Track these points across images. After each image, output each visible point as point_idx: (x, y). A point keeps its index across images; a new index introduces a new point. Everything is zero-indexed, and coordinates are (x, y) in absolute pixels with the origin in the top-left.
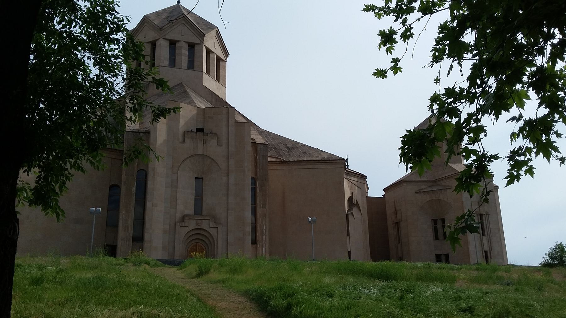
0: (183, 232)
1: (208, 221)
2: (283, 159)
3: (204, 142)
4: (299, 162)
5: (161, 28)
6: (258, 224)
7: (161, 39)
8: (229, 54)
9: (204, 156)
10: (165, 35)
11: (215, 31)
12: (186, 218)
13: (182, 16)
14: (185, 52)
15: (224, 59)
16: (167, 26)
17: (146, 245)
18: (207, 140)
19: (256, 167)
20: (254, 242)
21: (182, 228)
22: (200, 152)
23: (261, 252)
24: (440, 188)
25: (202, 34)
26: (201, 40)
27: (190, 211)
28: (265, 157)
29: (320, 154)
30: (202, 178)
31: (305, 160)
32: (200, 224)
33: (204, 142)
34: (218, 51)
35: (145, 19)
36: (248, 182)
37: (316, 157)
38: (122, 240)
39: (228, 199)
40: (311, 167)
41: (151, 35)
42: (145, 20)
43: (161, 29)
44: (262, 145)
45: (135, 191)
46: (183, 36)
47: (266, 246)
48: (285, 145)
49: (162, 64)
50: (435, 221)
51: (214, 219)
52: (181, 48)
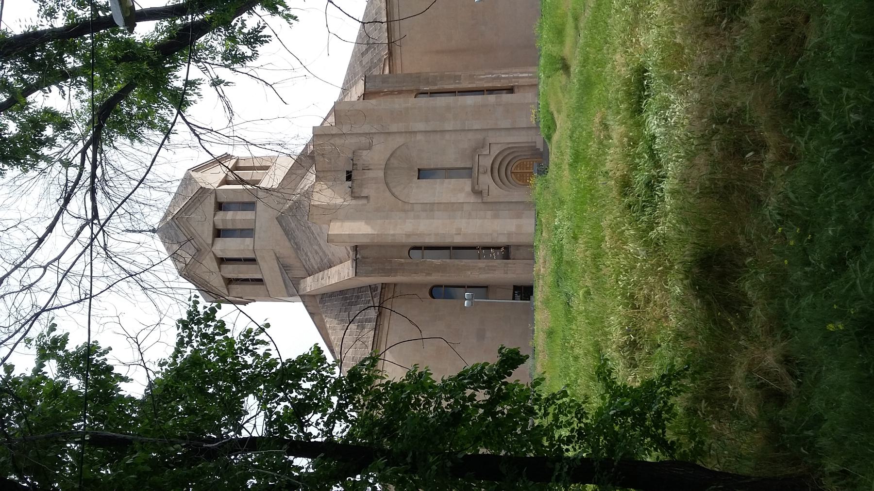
0: (496, 192)
2: (386, 55)
3: (366, 168)
5: (198, 251)
6: (485, 86)
7: (213, 249)
8: (226, 154)
9: (387, 168)
10: (208, 245)
11: (194, 174)
12: (476, 188)
14: (229, 215)
15: (235, 160)
17: (514, 240)
18: (363, 164)
19: (400, 92)
20: (511, 90)
22: (381, 174)
23: (524, 80)
25: (200, 191)
27: (466, 184)
28: (384, 79)
30: (419, 170)
32: (485, 169)
33: (366, 168)
36: (423, 101)
38: (507, 273)
41: (209, 263)
47: (516, 73)
48: (363, 54)
49: (251, 248)
52: (224, 221)
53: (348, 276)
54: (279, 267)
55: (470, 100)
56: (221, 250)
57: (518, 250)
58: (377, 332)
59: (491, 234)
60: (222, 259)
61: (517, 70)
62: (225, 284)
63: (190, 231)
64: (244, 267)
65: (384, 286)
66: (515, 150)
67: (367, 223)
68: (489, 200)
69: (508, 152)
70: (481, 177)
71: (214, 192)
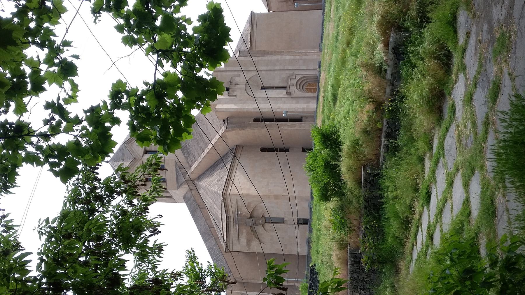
0: (298, 93)
3: (236, 84)
4: (251, 42)
7: (143, 158)
10: (140, 156)
12: (289, 91)
16: (132, 154)
33: (236, 84)
39: (277, 70)
40: (255, 34)
43: (135, 159)
45: (269, 122)
51: (289, 77)
54: (176, 169)
57: (306, 119)
59: (295, 108)
61: (310, 50)
63: (132, 150)
65: (237, 146)
66: (308, 78)
67: (234, 105)
68: (294, 96)
69: (304, 79)
70: (291, 88)
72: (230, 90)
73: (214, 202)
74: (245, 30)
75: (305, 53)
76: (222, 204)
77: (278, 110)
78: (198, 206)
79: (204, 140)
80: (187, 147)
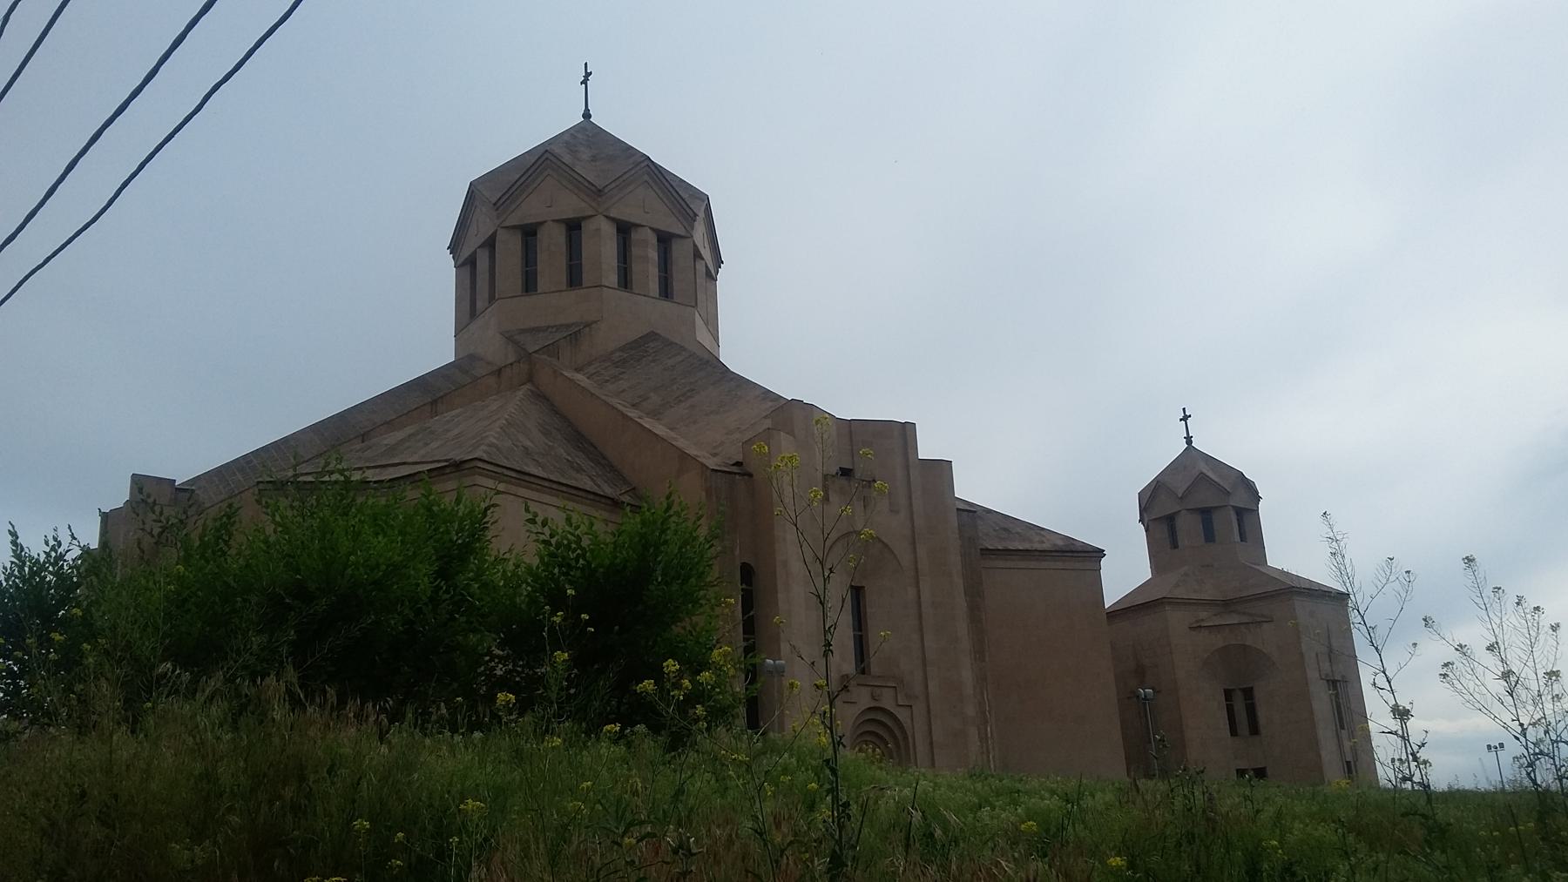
1: (891, 689)
3: (866, 502)
4: (1007, 553)
5: (600, 191)
7: (603, 218)
13: (646, 163)
14: (653, 254)
16: (613, 185)
21: (846, 705)
24: (1245, 619)
26: (689, 229)
29: (1044, 536)
30: (864, 587)
31: (1021, 548)
33: (866, 502)
34: (706, 253)
35: (547, 159)
37: (1039, 542)
40: (1033, 564)
41: (570, 205)
42: (549, 162)
43: (600, 193)
44: (966, 513)
46: (648, 213)
49: (603, 284)
50: (1228, 694)
53: (697, 456)
54: (568, 326)
55: (967, 675)
56: (598, 230)
58: (591, 497)
60: (579, 227)
62: (527, 225)
64: (562, 262)
71: (689, 235)
72: (843, 481)
73: (453, 440)
74: (1042, 532)
75: (987, 735)
76: (438, 461)
77: (785, 648)
78: (442, 397)
79: (671, 407)
80: (645, 357)
